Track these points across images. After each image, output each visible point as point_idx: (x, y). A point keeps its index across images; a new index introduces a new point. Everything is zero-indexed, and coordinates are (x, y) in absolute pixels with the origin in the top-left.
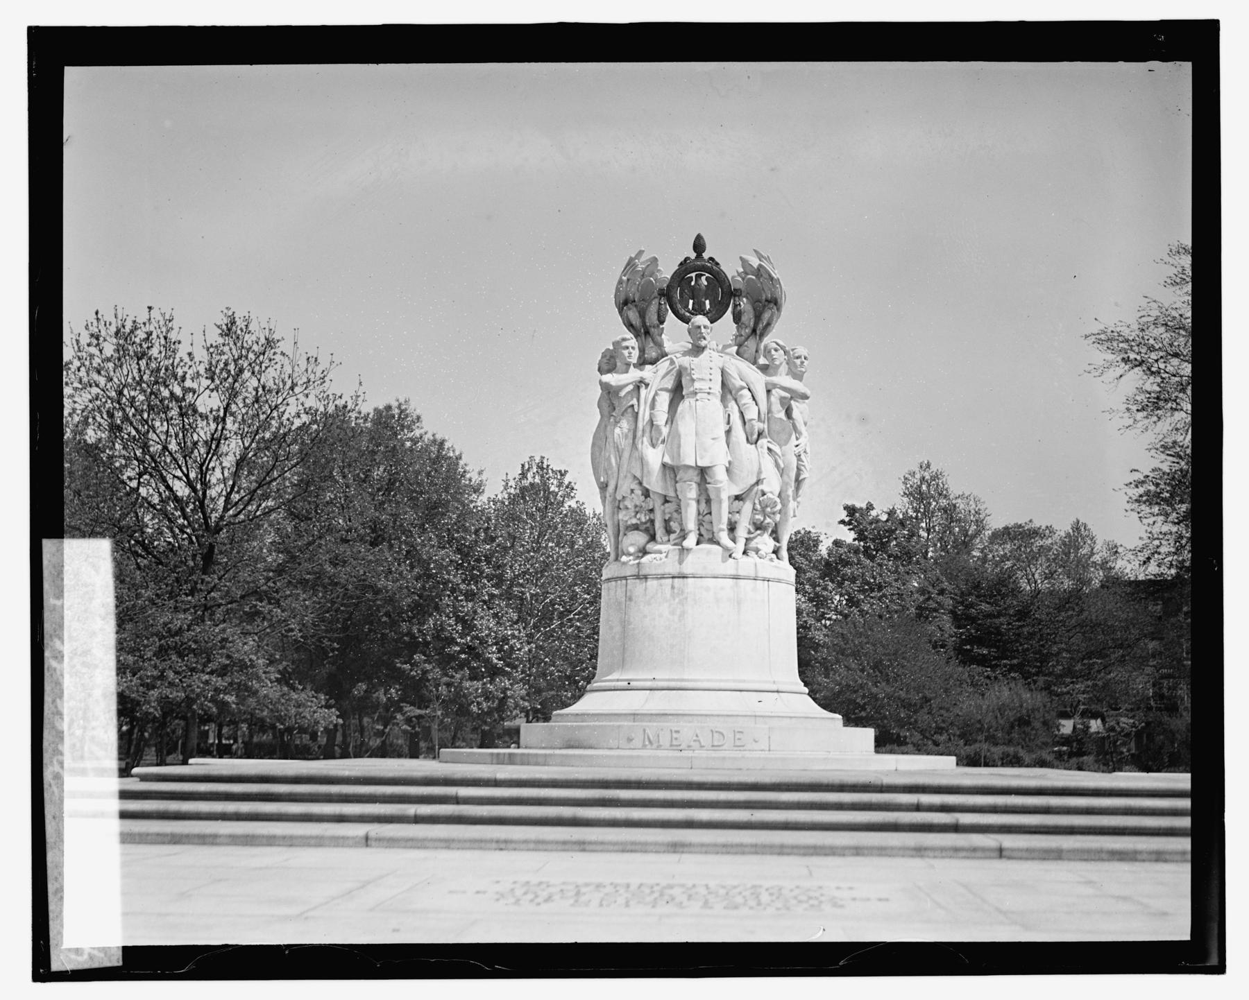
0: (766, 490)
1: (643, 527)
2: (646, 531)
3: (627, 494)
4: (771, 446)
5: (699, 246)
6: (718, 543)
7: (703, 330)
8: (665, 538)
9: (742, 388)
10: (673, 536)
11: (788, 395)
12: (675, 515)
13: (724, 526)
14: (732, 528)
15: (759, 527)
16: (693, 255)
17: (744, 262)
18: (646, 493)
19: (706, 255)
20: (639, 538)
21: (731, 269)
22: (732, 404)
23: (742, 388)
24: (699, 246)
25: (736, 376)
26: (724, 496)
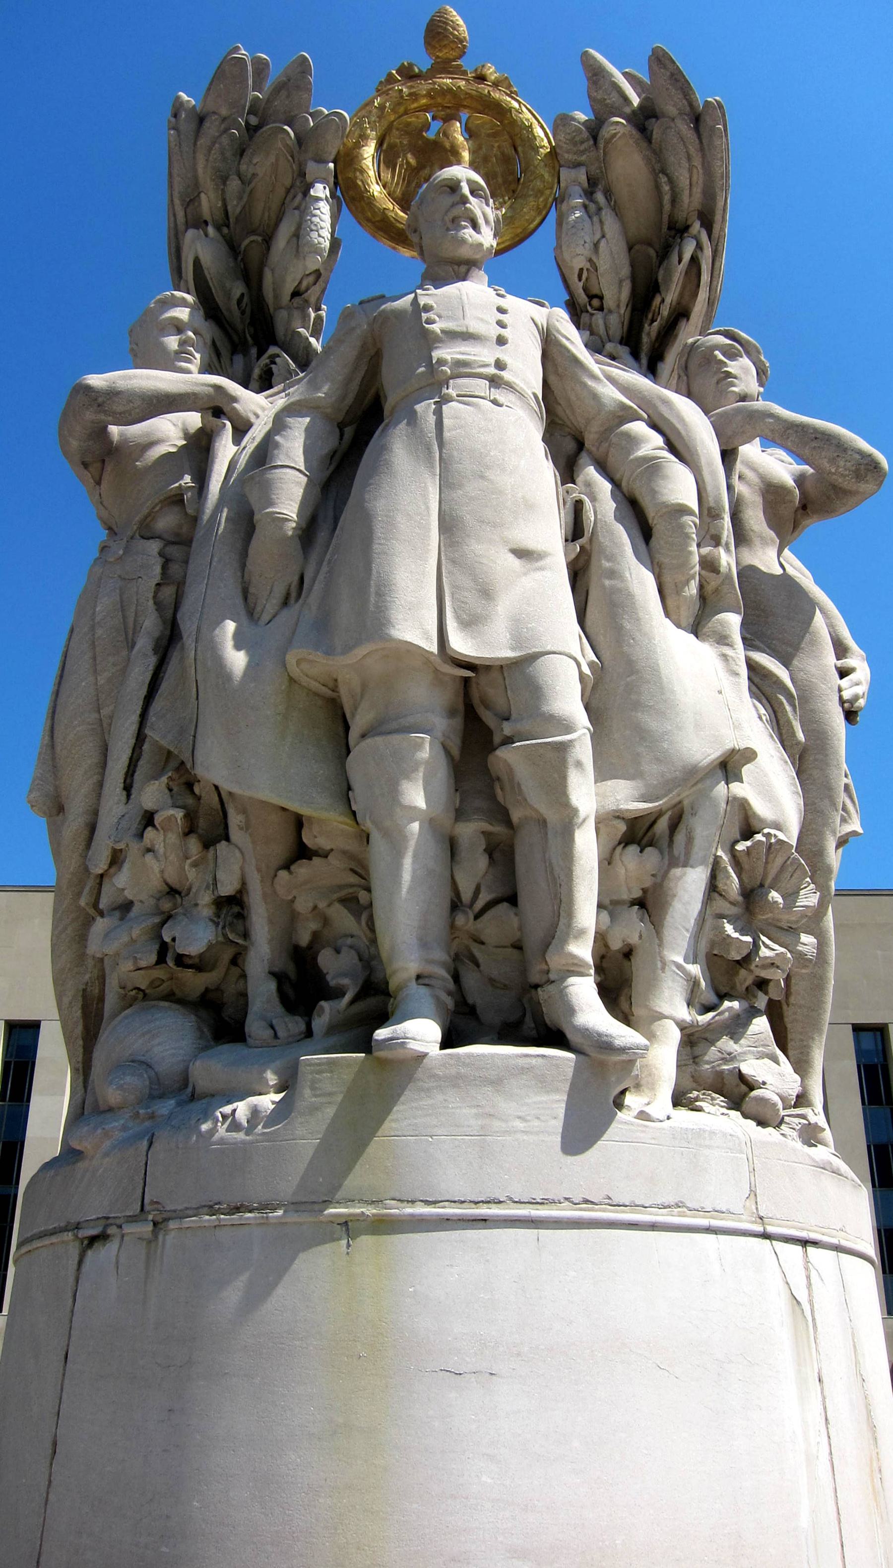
0: (761, 808)
1: (195, 982)
6: (554, 1036)
8: (296, 1025)
9: (625, 415)
13: (583, 950)
18: (209, 825)
20: (167, 1038)
22: (591, 472)
23: (625, 415)
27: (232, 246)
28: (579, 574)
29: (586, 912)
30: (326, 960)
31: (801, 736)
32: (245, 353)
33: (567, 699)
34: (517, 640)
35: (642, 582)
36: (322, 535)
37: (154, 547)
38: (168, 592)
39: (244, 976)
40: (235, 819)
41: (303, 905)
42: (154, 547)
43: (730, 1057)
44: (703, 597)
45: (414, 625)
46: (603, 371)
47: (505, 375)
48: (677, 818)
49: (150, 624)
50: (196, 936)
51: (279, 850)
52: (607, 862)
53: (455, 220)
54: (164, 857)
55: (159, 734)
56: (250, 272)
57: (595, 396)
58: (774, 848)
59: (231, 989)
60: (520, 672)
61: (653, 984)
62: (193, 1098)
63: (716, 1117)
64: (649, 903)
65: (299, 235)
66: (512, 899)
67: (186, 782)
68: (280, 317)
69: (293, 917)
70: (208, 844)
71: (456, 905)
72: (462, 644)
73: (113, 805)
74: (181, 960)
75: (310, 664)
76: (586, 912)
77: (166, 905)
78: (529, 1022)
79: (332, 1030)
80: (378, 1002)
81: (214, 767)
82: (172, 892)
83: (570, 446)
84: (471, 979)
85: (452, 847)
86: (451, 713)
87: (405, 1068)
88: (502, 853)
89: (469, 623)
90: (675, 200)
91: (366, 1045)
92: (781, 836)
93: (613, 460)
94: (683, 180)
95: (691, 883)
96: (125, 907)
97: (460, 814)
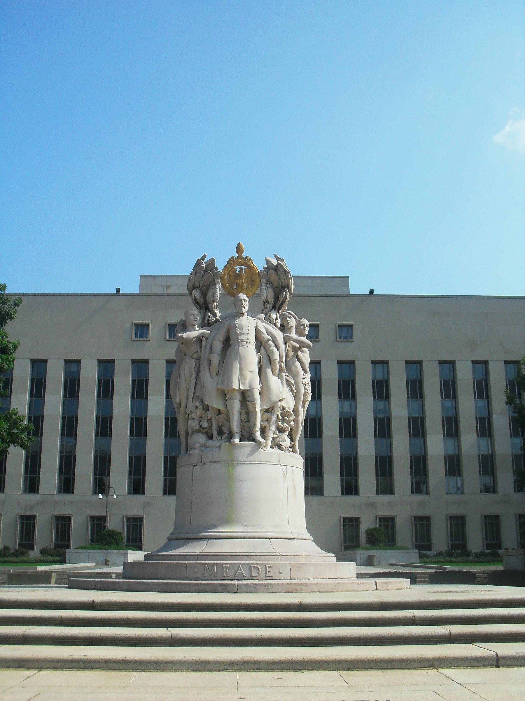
0: (285, 406)
1: (204, 430)
2: (206, 433)
3: (194, 409)
4: (288, 379)
5: (239, 249)
6: (254, 440)
7: (244, 302)
8: (219, 438)
9: (269, 340)
10: (224, 436)
11: (297, 345)
12: (226, 423)
13: (258, 429)
14: (263, 431)
15: (281, 430)
16: (236, 255)
17: (267, 261)
18: (206, 408)
19: (244, 256)
20: (201, 439)
21: (259, 265)
24: (239, 249)
25: (264, 331)
26: (258, 408)
27: (200, 290)
28: (260, 369)
29: (259, 423)
30: (223, 428)
31: (295, 391)
32: (203, 309)
33: (257, 396)
34: (250, 387)
35: (269, 371)
36: (221, 364)
37: (194, 360)
38: (196, 368)
39: (211, 429)
40: (210, 408)
41: (220, 420)
42: (194, 360)
43: (279, 441)
44: (279, 370)
45: (236, 387)
46: (266, 329)
47: (248, 341)
48: (273, 408)
49: (194, 374)
50: (205, 425)
51: (216, 413)
52: (262, 416)
53: (242, 307)
54: (200, 412)
55: (198, 394)
56: (204, 295)
57: (264, 337)
58: (287, 412)
59: (209, 431)
60: (251, 390)
61: (269, 432)
62: (206, 447)
63: (276, 450)
64: (268, 421)
65: (214, 294)
66: (249, 421)
67: (202, 402)
68: (210, 306)
69: (219, 422)
70: (206, 411)
71: (241, 422)
72: (242, 388)
73: (190, 404)
74: (203, 428)
75: (220, 386)
76: (259, 423)
77: (200, 419)
78: (251, 438)
79: (226, 438)
80: (231, 436)
81: (207, 402)
82: (201, 417)
83: (260, 344)
84: (243, 432)
85: (241, 413)
86: (241, 395)
87: (234, 444)
88: (248, 413)
89: (243, 384)
90: (282, 283)
91: (229, 441)
92: (289, 410)
93: (266, 348)
94: (283, 281)
95: (274, 417)
96: (193, 419)
97: (242, 409)
